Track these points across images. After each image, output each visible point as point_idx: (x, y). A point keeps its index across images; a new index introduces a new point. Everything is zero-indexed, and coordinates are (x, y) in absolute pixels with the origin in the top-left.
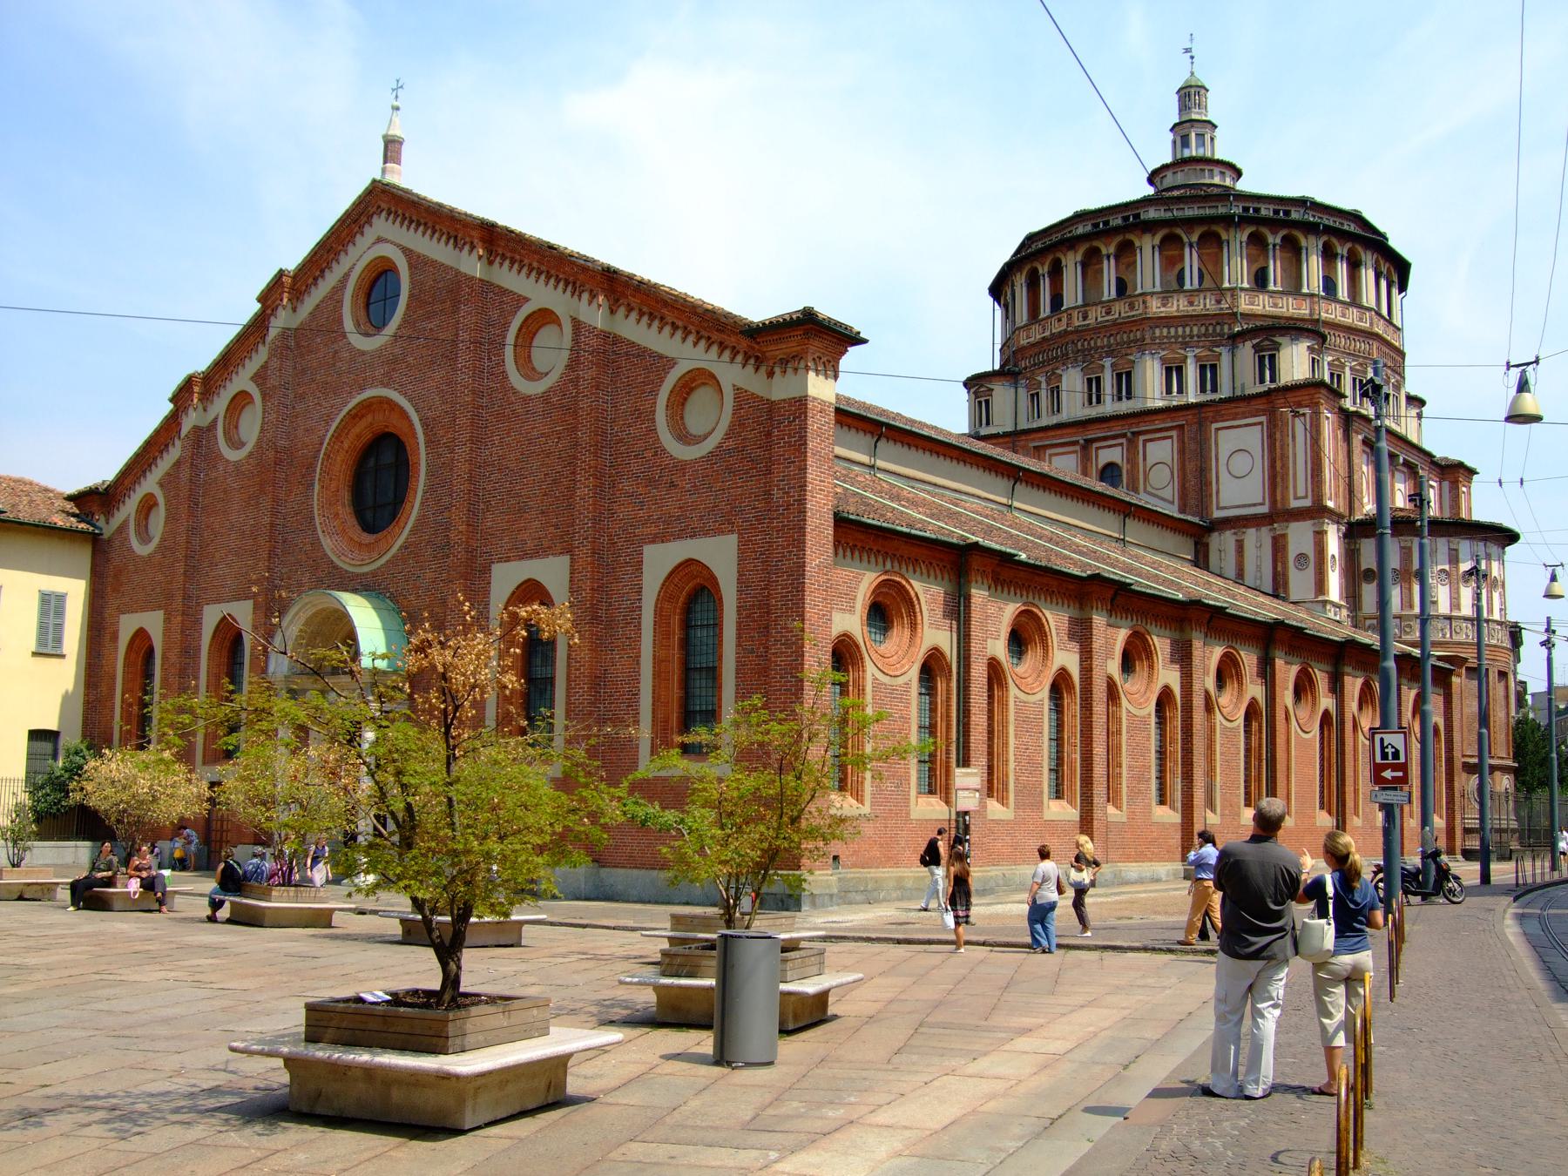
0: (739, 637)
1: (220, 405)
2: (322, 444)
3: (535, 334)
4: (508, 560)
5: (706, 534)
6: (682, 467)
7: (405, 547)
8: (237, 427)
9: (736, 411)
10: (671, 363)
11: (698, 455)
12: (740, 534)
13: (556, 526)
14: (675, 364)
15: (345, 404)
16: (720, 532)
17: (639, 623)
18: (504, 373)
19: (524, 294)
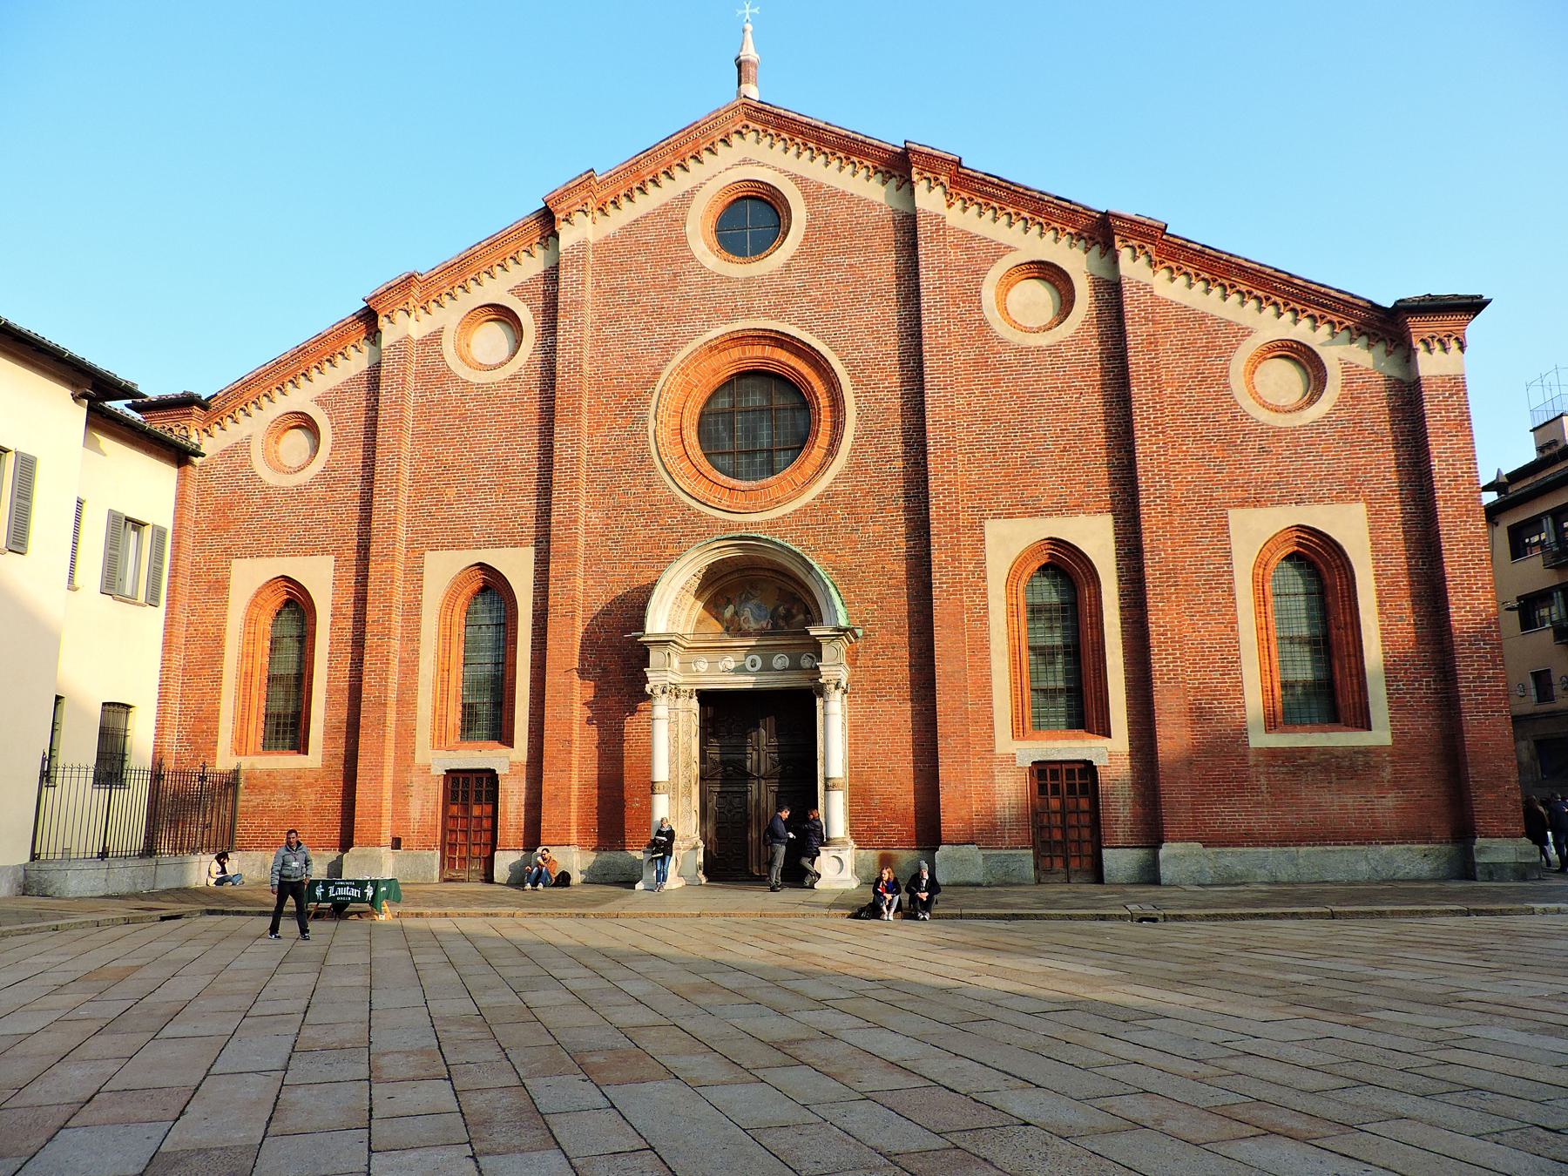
0: (1381, 604)
1: (449, 315)
2: (657, 374)
3: (1012, 286)
4: (1010, 516)
5: (1320, 501)
6: (1278, 433)
7: (828, 495)
8: (468, 346)
9: (1347, 383)
10: (1248, 332)
11: (1298, 424)
12: (1369, 503)
13: (1087, 484)
14: (1252, 332)
15: (696, 334)
16: (1338, 499)
17: (1231, 589)
18: (983, 324)
19: (1007, 243)
